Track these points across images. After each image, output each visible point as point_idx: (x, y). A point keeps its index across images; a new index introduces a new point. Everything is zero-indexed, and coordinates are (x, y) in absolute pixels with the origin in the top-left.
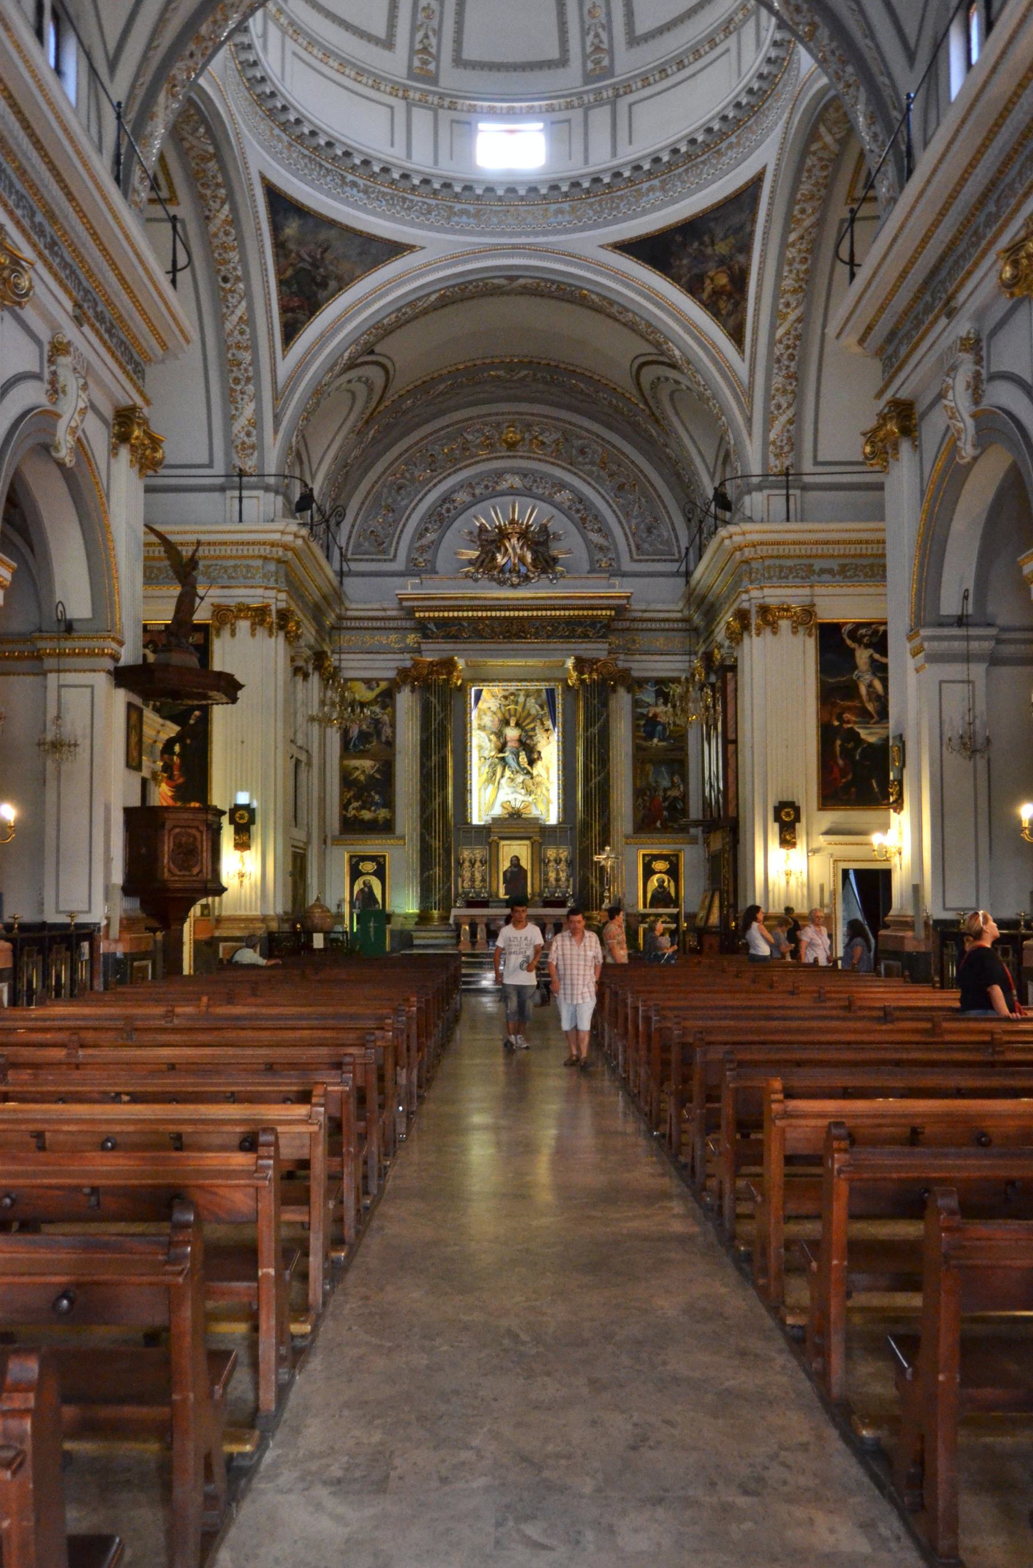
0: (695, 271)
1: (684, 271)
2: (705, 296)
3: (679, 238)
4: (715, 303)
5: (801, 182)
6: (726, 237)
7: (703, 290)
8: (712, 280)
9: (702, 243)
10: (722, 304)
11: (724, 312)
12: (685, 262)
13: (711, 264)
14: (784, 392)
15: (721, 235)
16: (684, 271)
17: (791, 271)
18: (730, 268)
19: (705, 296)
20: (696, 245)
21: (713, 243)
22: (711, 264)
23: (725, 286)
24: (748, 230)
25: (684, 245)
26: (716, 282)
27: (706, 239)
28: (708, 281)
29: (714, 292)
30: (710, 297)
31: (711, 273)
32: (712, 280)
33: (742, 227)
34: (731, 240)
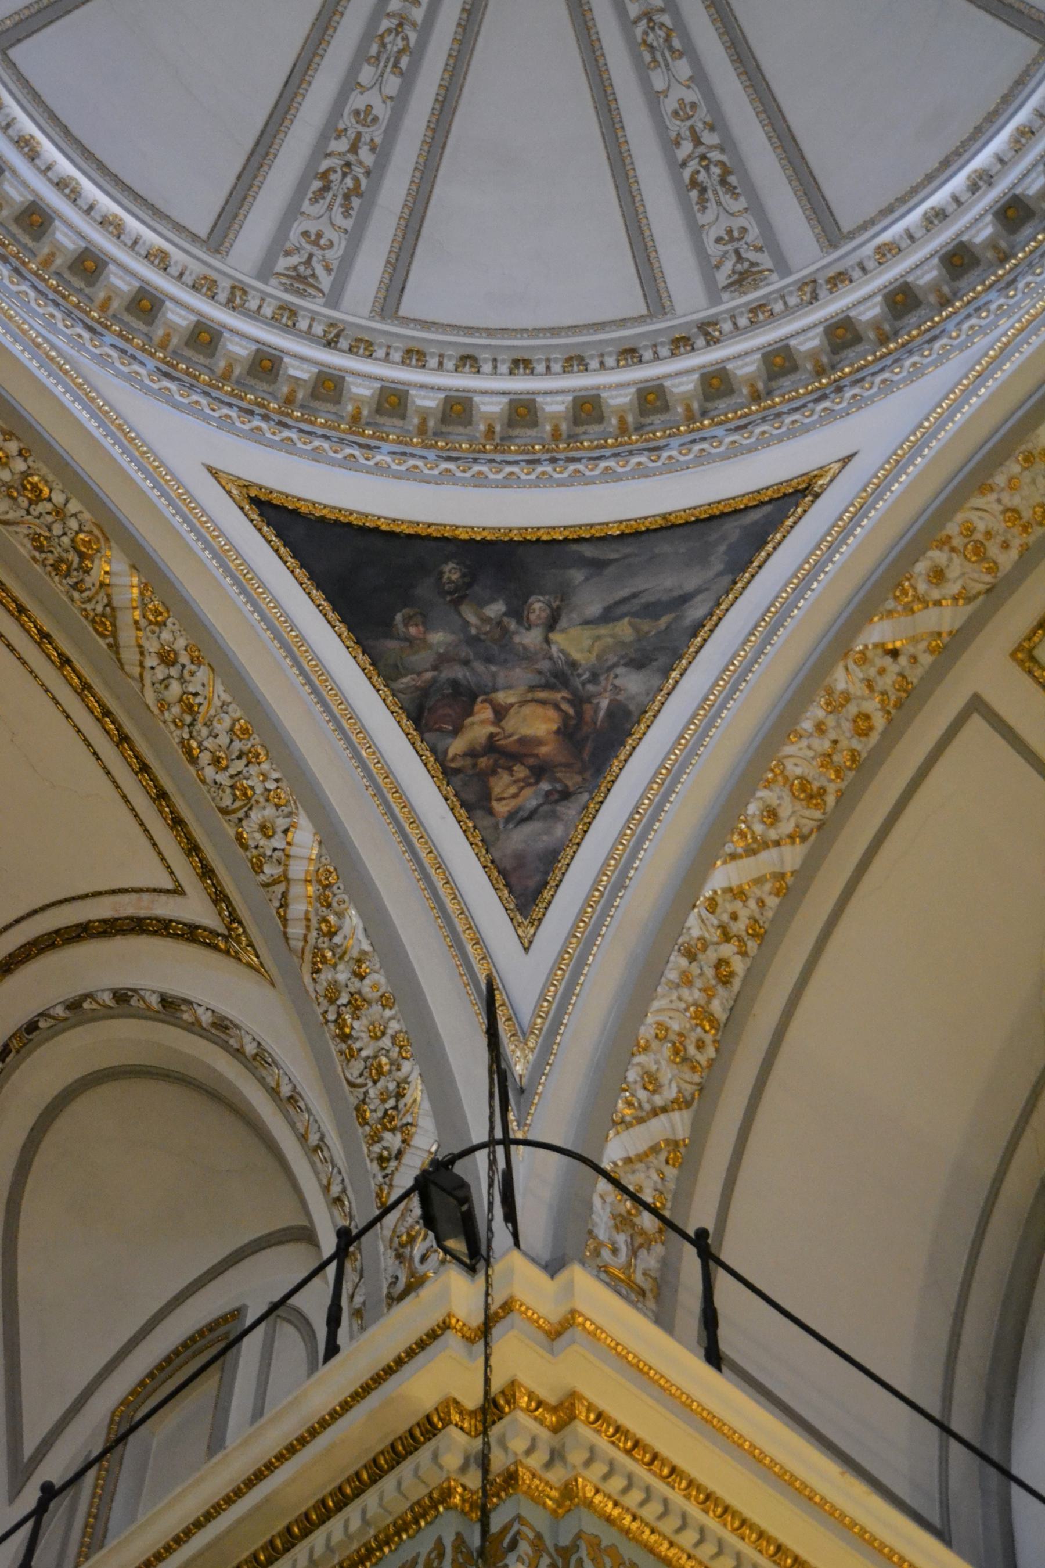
0: (458, 673)
1: (422, 658)
2: (457, 746)
3: (452, 572)
4: (484, 777)
5: (985, 488)
6: (608, 616)
7: (456, 731)
8: (500, 713)
9: (518, 612)
10: (502, 784)
11: (501, 809)
12: (437, 637)
13: (521, 675)
14: (681, 1057)
15: (594, 609)
16: (422, 658)
17: (820, 728)
18: (579, 701)
19: (457, 746)
20: (496, 609)
21: (552, 623)
22: (521, 675)
23: (538, 742)
24: (695, 612)
25: (459, 596)
26: (511, 723)
27: (538, 607)
28: (484, 712)
29: (491, 746)
30: (472, 753)
31: (502, 697)
32: (500, 713)
33: (684, 599)
34: (624, 629)
